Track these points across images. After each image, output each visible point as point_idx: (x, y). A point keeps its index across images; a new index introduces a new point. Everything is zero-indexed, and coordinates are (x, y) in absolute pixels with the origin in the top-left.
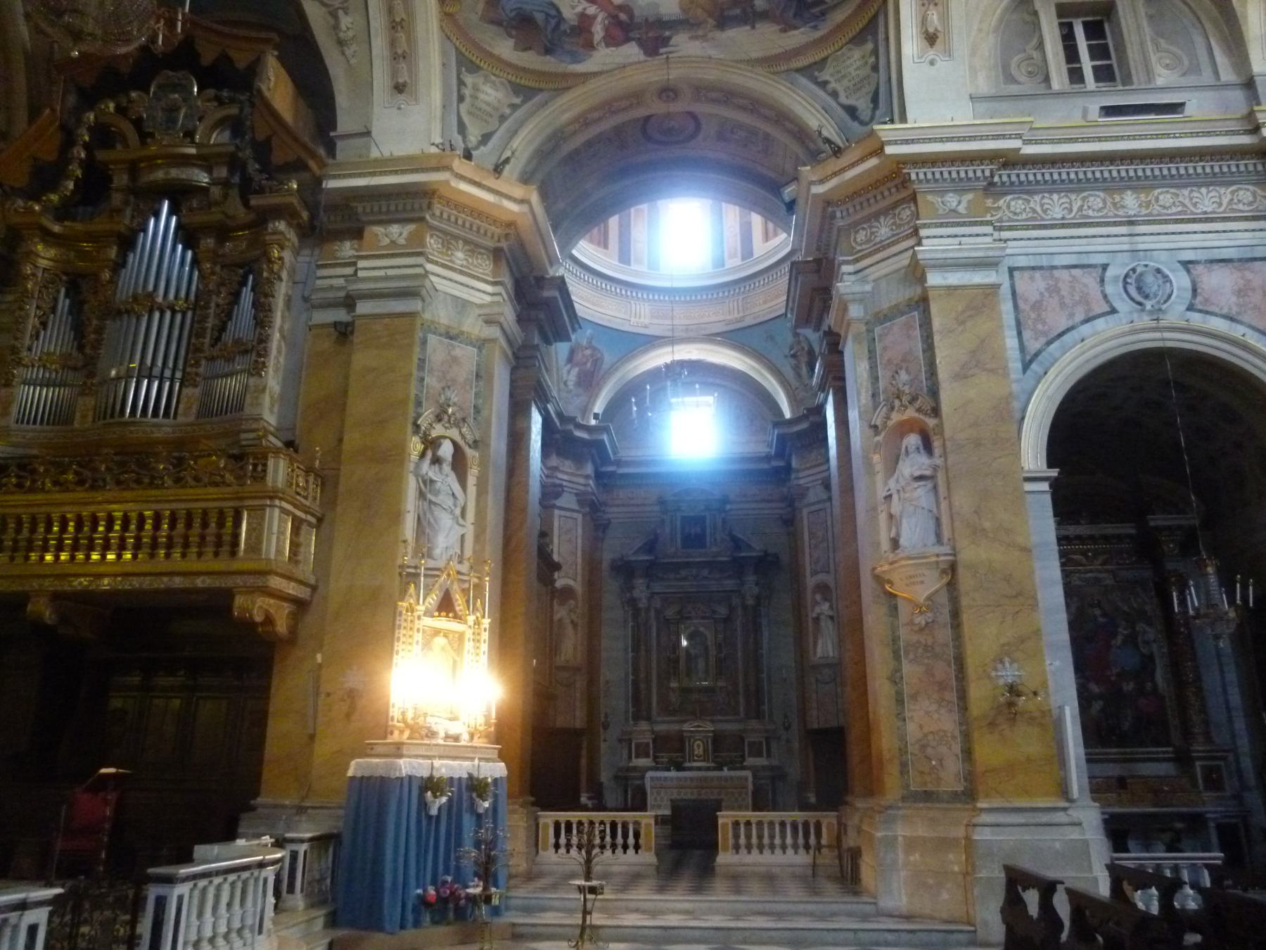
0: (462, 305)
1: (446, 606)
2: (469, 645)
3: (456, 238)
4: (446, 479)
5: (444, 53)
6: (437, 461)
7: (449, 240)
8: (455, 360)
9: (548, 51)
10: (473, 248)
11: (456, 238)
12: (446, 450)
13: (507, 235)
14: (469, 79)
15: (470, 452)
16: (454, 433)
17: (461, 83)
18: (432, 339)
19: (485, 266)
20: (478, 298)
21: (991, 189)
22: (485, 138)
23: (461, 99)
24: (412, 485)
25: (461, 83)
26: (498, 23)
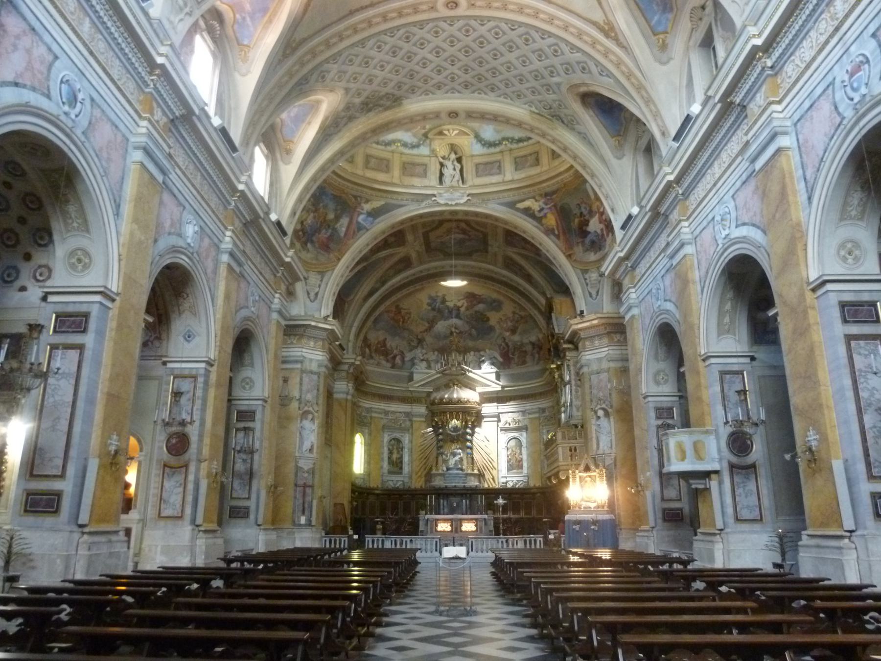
0: (600, 360)
1: (587, 469)
2: (598, 479)
3: (594, 337)
4: (604, 422)
5: (577, 274)
6: (599, 418)
7: (591, 338)
8: (601, 380)
9: (600, 249)
10: (600, 336)
11: (594, 337)
12: (601, 413)
13: (606, 328)
14: (587, 276)
15: (610, 410)
16: (604, 406)
17: (585, 279)
18: (593, 377)
19: (605, 340)
20: (603, 355)
21: (634, 268)
22: (598, 292)
23: (587, 285)
24: (594, 428)
25: (585, 279)
26: (587, 250)
